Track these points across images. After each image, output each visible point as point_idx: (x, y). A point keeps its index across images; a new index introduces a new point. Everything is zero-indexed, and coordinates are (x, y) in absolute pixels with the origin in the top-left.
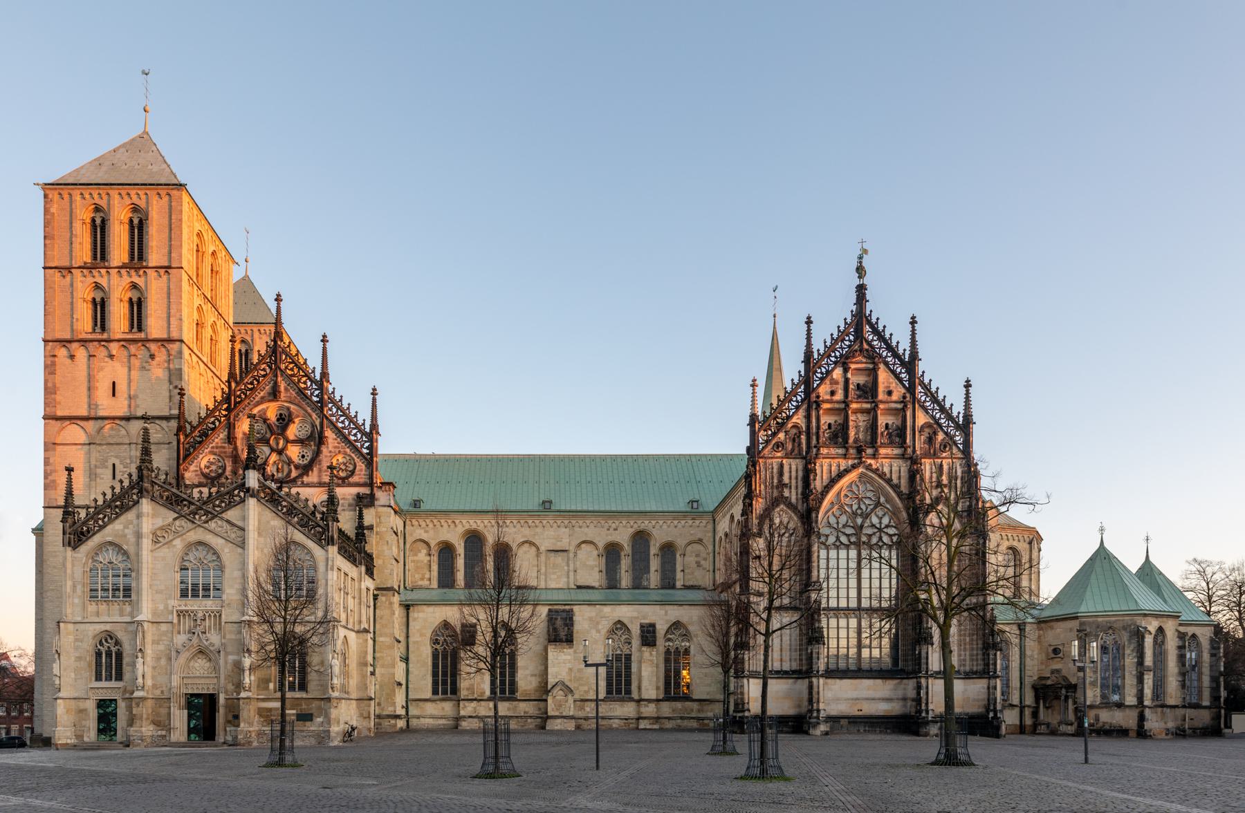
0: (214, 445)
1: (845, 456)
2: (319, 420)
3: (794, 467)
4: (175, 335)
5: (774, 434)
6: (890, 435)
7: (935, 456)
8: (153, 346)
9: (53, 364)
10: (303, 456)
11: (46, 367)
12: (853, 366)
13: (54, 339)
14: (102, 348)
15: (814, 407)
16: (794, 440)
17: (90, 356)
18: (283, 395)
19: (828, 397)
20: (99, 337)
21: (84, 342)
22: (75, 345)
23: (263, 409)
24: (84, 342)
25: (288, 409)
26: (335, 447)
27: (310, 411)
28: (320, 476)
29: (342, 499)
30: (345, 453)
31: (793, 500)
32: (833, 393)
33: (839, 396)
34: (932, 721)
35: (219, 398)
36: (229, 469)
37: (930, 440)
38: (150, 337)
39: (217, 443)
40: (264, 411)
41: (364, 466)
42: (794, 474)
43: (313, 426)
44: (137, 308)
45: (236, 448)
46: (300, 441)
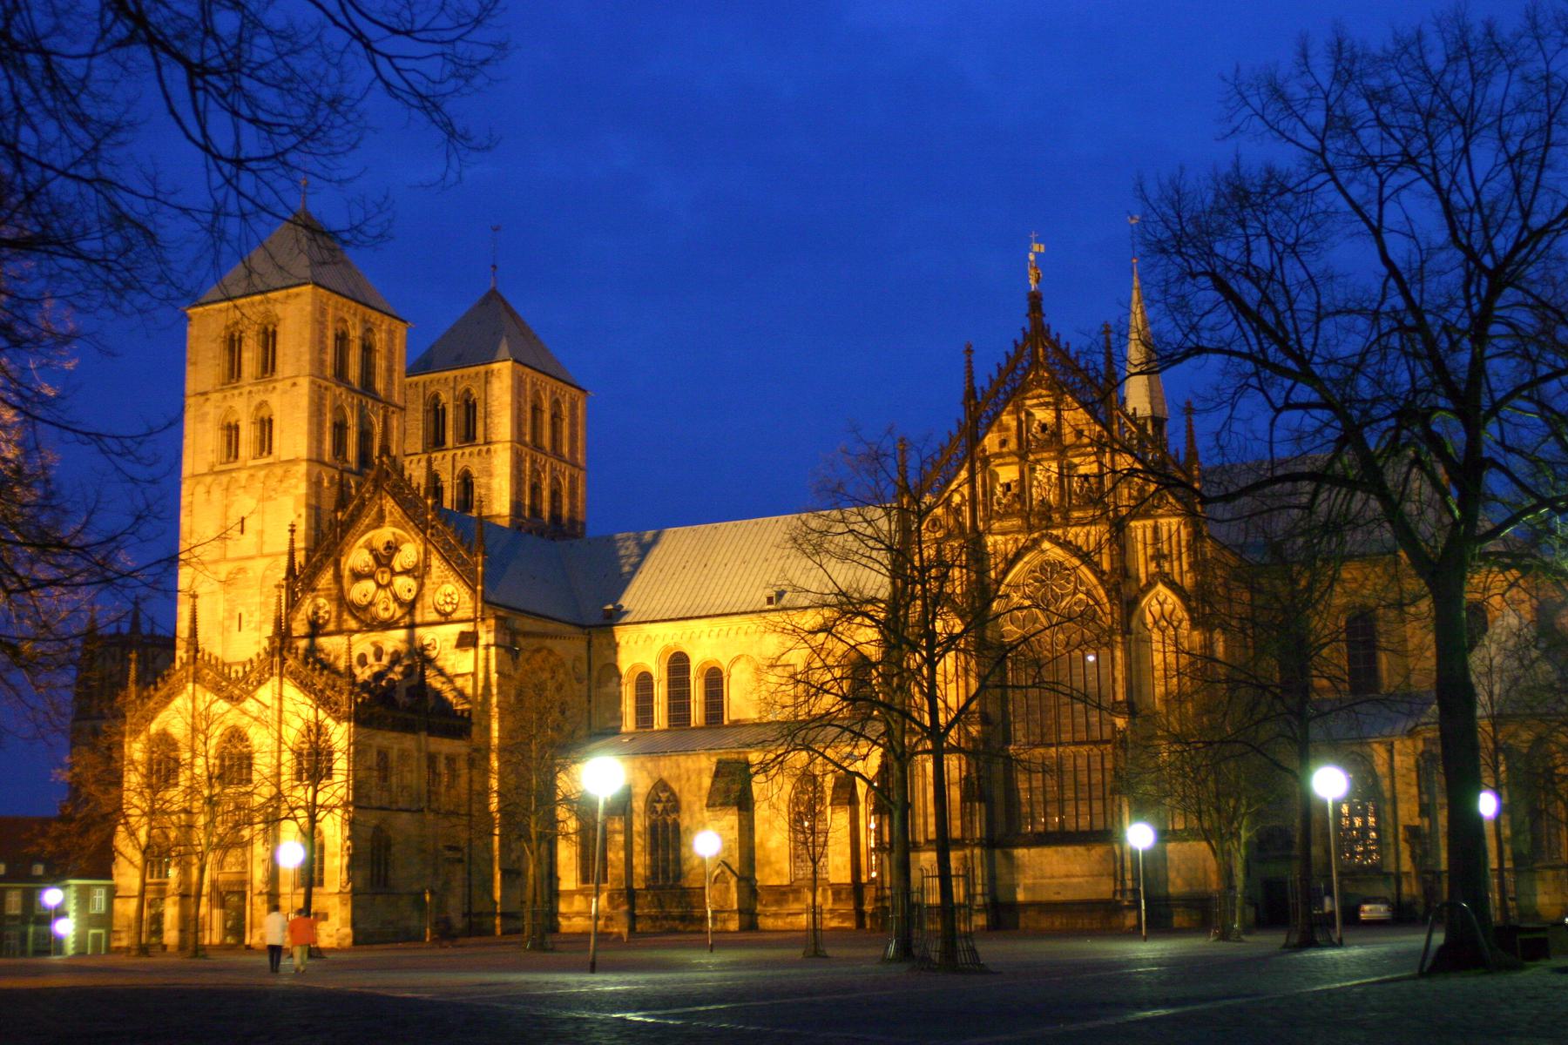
8: (279, 471)
10: (410, 591)
15: (978, 464)
18: (387, 519)
19: (996, 449)
22: (209, 479)
25: (394, 534)
26: (439, 577)
28: (423, 615)
29: (446, 640)
32: (1003, 443)
33: (1013, 445)
34: (1127, 907)
44: (266, 426)
45: (341, 589)
46: (406, 572)
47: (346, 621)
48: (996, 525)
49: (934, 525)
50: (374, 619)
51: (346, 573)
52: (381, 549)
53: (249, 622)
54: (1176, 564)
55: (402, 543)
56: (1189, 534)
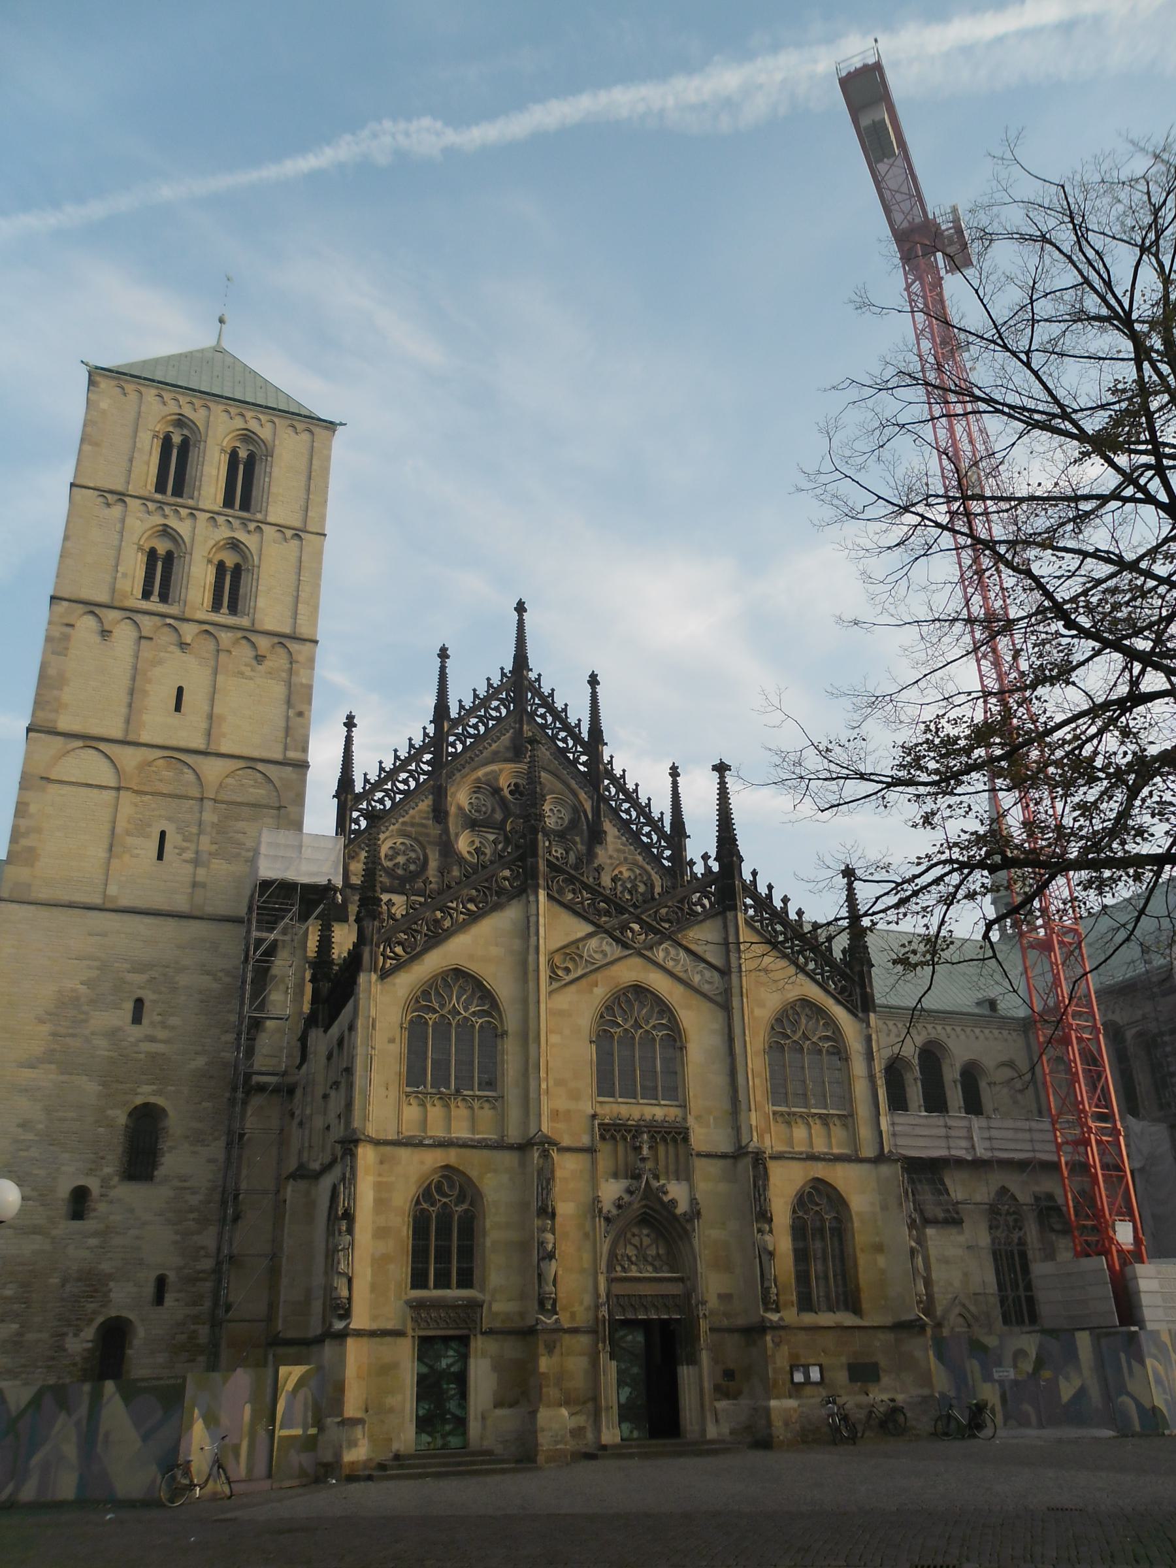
0: (406, 819)
2: (590, 803)
4: (304, 631)
8: (263, 643)
9: (66, 638)
11: (49, 639)
13: (73, 597)
14: (166, 630)
17: (141, 638)
20: (162, 608)
21: (131, 613)
23: (495, 771)
24: (131, 613)
26: (618, 851)
30: (635, 864)
35: (418, 742)
36: (433, 864)
38: (258, 627)
39: (413, 817)
40: (496, 775)
43: (577, 810)
45: (446, 831)
51: (453, 810)
52: (506, 792)
53: (183, 850)
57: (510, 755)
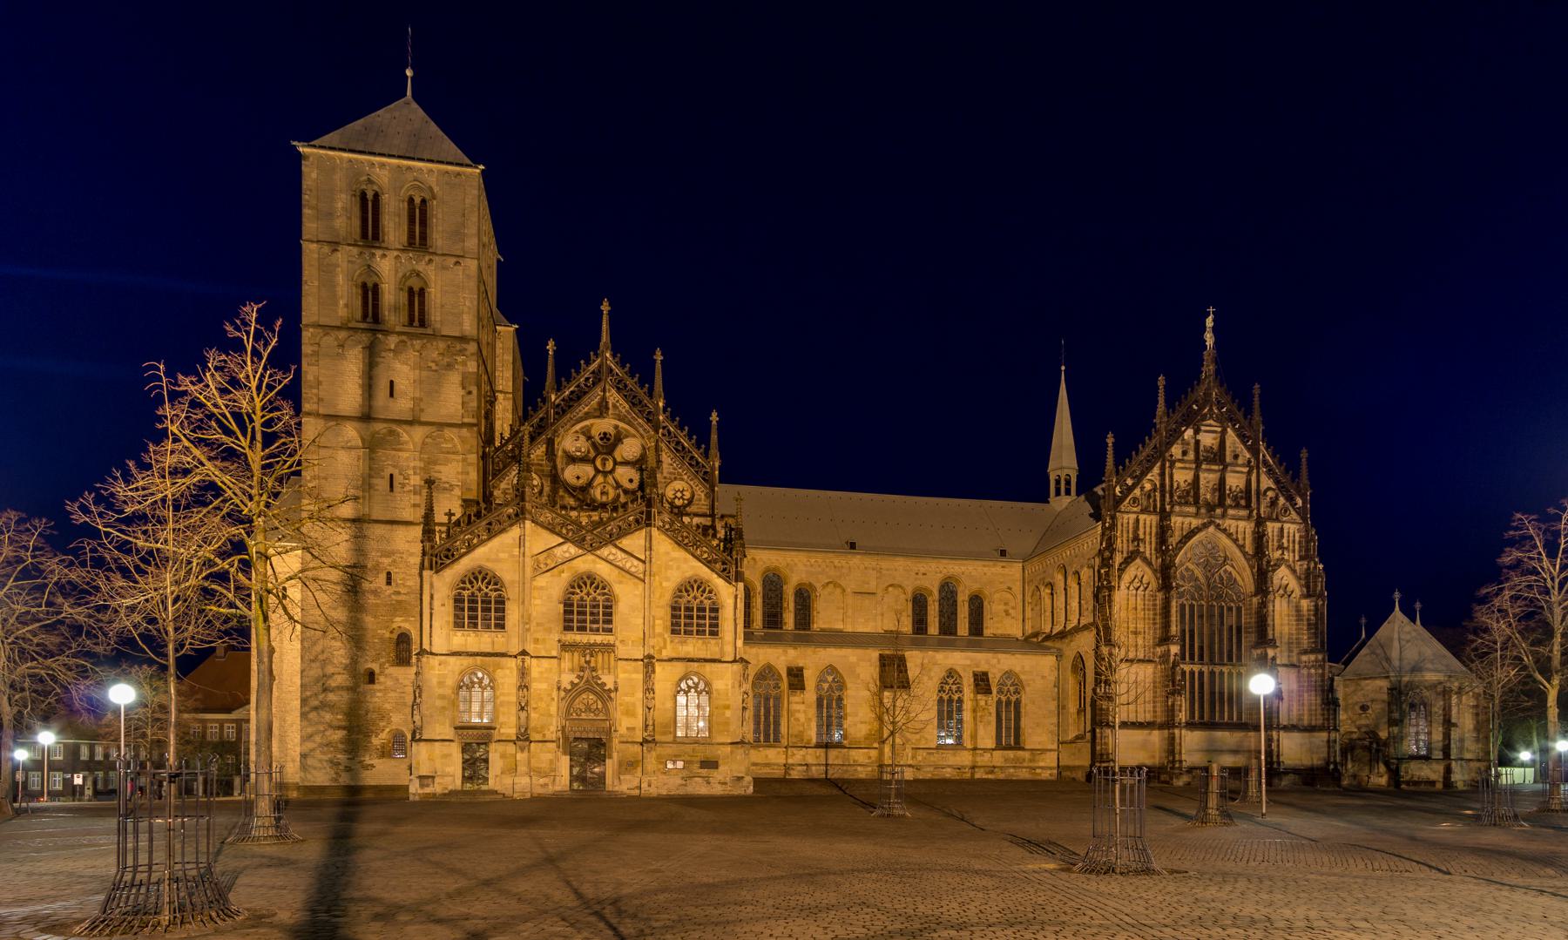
1: (1197, 515)
3: (1148, 523)
5: (1130, 489)
6: (1235, 499)
7: (1277, 520)
10: (631, 481)
12: (1203, 428)
15: (1167, 464)
16: (1149, 497)
25: (616, 427)
26: (671, 473)
27: (642, 432)
31: (1148, 555)
32: (1184, 453)
33: (1191, 456)
37: (1273, 503)
41: (703, 495)
42: (1148, 530)
45: (555, 467)
47: (562, 497)
48: (1177, 508)
49: (1134, 502)
50: (594, 500)
51: (560, 453)
52: (597, 439)
54: (1291, 554)
55: (627, 437)
56: (1300, 537)
57: (597, 414)
